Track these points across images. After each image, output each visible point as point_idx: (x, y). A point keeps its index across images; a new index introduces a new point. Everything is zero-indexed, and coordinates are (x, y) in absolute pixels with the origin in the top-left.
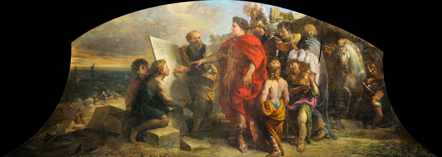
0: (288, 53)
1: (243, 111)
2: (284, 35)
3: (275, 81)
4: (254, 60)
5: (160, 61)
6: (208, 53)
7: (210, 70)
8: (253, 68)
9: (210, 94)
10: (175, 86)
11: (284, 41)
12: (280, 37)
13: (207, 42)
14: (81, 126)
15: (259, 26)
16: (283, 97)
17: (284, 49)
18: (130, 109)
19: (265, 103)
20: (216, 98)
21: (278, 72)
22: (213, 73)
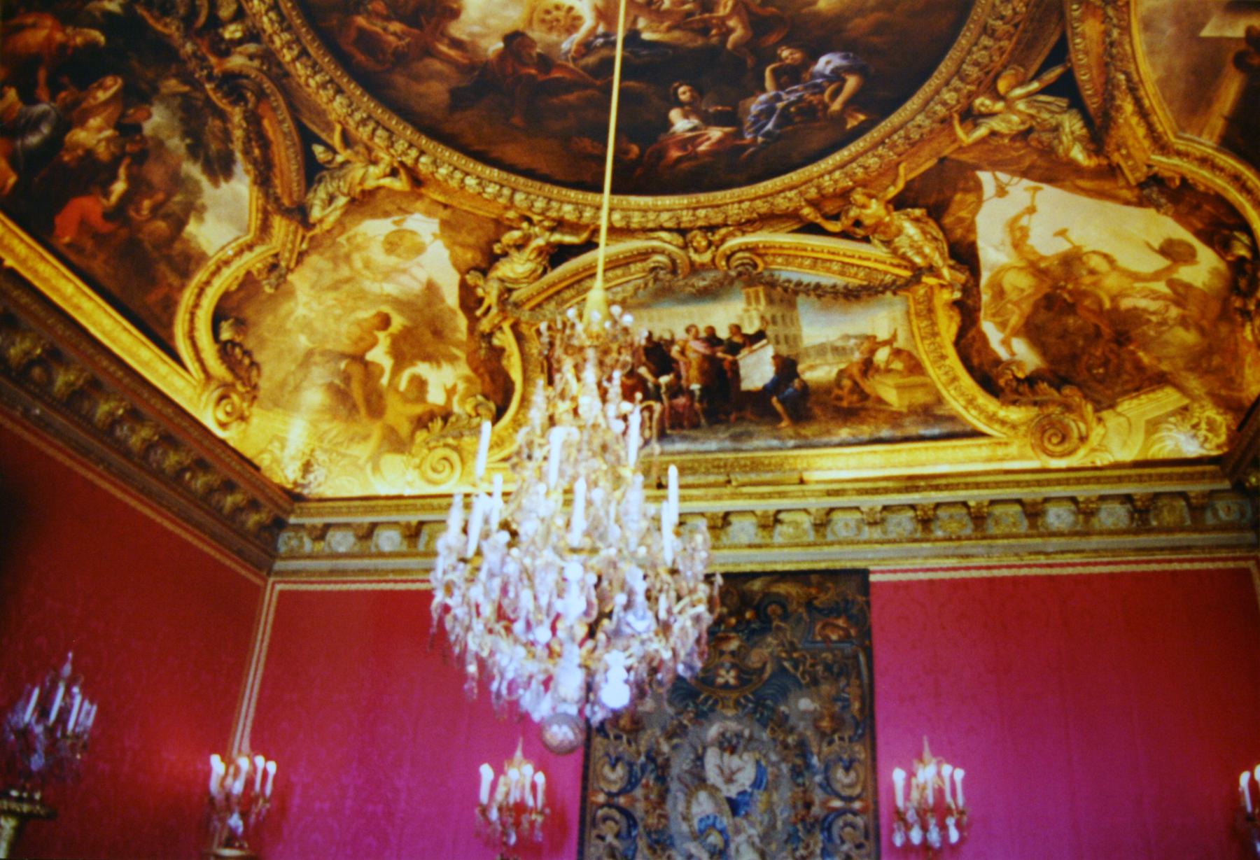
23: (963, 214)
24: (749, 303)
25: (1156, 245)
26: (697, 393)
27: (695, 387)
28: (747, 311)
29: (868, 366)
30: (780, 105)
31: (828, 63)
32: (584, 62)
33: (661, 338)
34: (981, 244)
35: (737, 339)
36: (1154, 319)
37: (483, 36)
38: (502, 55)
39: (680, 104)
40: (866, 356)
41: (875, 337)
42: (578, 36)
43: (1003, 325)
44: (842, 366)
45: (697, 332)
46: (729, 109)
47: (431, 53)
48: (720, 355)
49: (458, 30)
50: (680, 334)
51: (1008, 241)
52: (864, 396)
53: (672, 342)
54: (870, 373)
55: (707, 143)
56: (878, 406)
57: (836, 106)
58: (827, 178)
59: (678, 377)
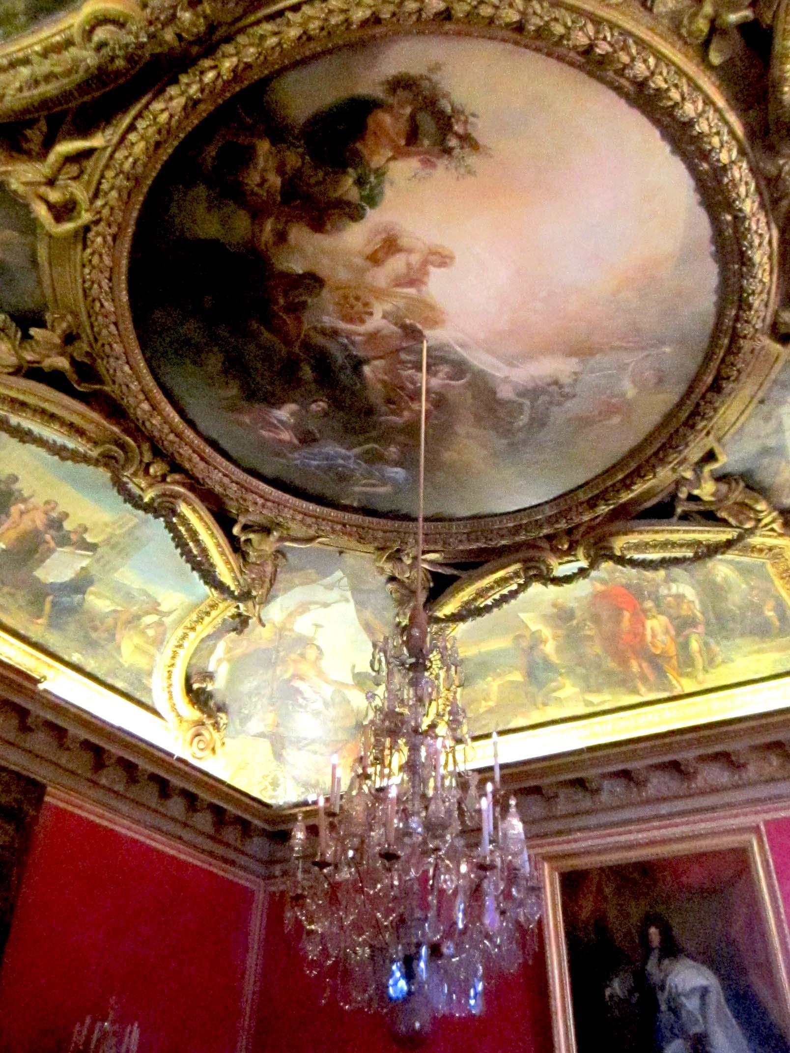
6: (578, 613)
10: (559, 650)
13: (573, 604)
14: (491, 704)
16: (667, 632)
17: (650, 589)
21: (654, 610)
22: (590, 629)
23: (297, 581)
24: (114, 523)
25: (356, 671)
28: (106, 525)
30: (341, 461)
32: (312, 333)
33: (20, 491)
34: (279, 600)
35: (74, 537)
39: (305, 407)
41: (159, 605)
42: (342, 325)
43: (229, 650)
44: (119, 608)
45: (53, 509)
47: (258, 214)
48: (48, 537)
50: (38, 501)
52: (112, 637)
53: (24, 500)
57: (357, 489)
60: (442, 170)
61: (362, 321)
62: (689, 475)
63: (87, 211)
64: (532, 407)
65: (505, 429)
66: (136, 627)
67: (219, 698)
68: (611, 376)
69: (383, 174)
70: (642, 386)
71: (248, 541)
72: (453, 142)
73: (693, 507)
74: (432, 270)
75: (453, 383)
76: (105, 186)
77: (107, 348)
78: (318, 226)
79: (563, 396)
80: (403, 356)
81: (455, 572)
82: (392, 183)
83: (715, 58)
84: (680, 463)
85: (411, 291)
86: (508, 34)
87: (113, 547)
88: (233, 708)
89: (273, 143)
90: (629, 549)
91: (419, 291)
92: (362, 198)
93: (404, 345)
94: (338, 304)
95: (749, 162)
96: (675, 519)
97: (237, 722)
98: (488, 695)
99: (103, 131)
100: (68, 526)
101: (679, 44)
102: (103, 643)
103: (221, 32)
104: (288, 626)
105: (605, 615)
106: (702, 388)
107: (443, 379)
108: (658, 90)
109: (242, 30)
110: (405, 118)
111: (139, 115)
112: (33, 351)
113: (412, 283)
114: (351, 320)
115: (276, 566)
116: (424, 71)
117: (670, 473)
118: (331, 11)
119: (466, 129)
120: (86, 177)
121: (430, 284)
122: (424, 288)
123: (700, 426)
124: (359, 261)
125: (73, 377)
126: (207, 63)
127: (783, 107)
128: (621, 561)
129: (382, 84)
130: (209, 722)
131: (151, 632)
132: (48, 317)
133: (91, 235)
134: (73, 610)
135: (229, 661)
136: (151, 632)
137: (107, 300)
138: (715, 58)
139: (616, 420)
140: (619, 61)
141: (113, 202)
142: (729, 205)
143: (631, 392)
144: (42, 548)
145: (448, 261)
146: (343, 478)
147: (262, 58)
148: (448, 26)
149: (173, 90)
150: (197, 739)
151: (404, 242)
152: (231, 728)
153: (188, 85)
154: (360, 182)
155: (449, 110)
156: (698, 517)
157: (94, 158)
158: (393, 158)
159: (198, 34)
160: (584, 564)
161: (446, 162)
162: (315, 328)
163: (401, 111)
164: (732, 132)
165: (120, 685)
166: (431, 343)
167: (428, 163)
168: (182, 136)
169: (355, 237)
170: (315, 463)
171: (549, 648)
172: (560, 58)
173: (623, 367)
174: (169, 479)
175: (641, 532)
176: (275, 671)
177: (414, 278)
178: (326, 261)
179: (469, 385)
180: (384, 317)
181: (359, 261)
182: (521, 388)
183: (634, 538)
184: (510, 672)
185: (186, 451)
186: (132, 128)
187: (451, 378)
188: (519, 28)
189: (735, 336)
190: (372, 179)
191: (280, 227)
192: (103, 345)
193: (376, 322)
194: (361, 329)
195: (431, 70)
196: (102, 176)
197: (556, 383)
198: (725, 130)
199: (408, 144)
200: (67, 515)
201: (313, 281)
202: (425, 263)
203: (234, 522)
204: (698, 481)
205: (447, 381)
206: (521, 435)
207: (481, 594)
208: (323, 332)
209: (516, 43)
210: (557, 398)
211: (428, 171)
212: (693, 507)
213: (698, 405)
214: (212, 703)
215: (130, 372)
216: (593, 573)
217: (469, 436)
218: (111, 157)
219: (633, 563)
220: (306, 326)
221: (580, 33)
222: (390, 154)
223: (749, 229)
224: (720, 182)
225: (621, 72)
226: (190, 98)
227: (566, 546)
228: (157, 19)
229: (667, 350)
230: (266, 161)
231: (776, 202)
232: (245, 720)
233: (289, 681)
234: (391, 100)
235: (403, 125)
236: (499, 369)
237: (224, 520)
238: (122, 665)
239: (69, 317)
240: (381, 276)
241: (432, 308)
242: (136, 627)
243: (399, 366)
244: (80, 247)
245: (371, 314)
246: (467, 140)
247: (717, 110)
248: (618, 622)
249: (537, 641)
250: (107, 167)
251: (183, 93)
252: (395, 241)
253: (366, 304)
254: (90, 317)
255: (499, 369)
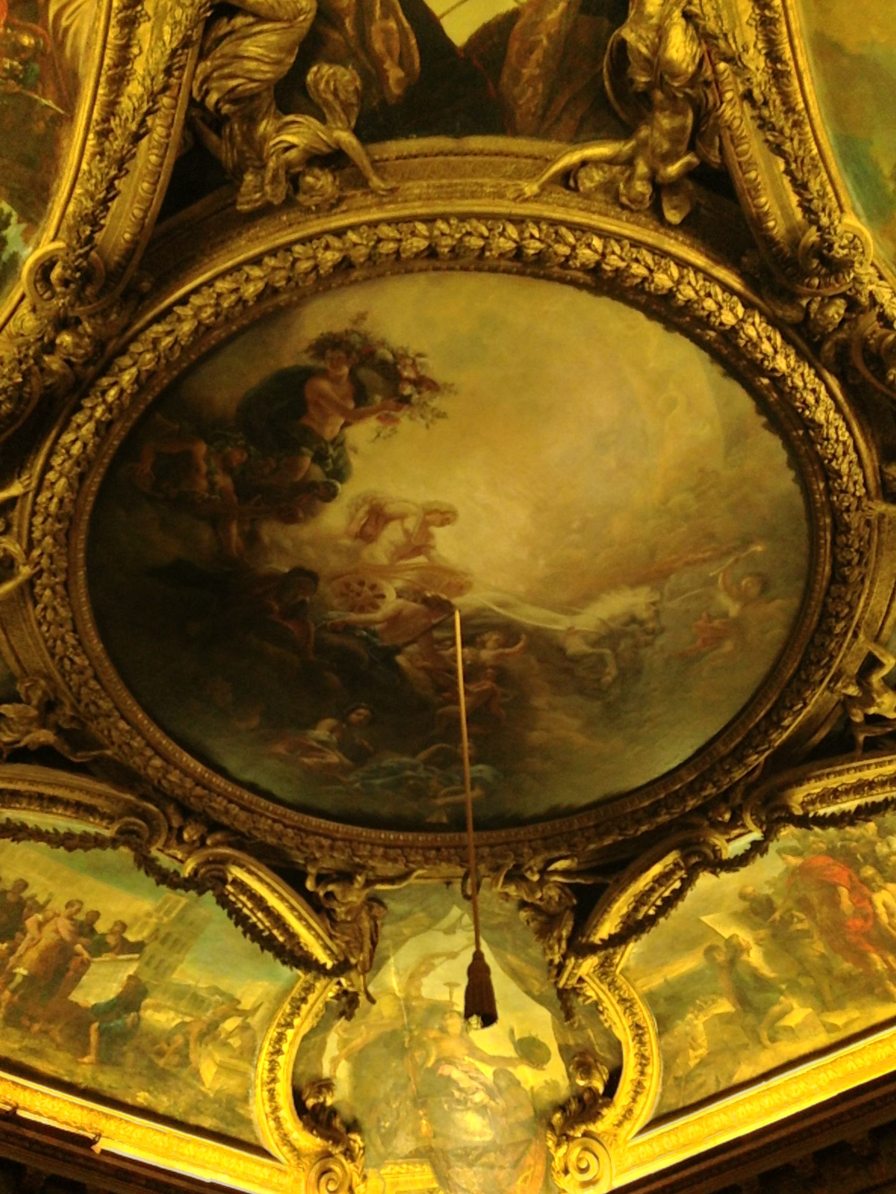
0: (874, 851)
1: (870, 948)
2: (853, 835)
3: (883, 891)
4: (836, 880)
5: (731, 937)
6: (778, 901)
7: (795, 920)
8: (844, 892)
9: (815, 946)
10: (769, 956)
11: (857, 841)
12: (850, 840)
13: (768, 891)
14: (702, 1052)
15: (814, 842)
17: (864, 850)
18: (739, 1007)
19: (889, 924)
20: (825, 947)
21: (878, 879)
22: (801, 921)
23: (406, 931)
24: (158, 910)
25: (517, 1037)
26: (18, 979)
27: (22, 971)
28: (149, 915)
29: (210, 1032)
30: (409, 773)
31: (481, 771)
34: (392, 960)
35: (111, 940)
36: (457, 1094)
37: (282, 550)
38: (274, 577)
39: (343, 717)
40: (216, 1018)
41: (239, 1002)
42: (354, 617)
43: (344, 1043)
44: (188, 1019)
45: (79, 910)
46: (371, 749)
47: (217, 521)
48: (79, 947)
49: (271, 531)
50: (58, 905)
51: (409, 972)
52: (185, 1061)
53: (41, 908)
54: (208, 1038)
55: (315, 760)
56: (190, 1080)
57: (440, 802)
58: (368, 847)
59: (12, 951)
60: (405, 422)
61: (376, 607)
62: (853, 691)
63: (25, 565)
64: (617, 656)
65: (591, 689)
66: (215, 1038)
67: (345, 1112)
68: (697, 597)
69: (342, 444)
70: (743, 598)
71: (330, 895)
72: (408, 390)
73: (878, 731)
74: (437, 531)
75: (507, 650)
76: (37, 535)
77: (93, 708)
78: (290, 517)
79: (648, 634)
80: (437, 634)
81: (600, 879)
82: (355, 451)
83: (673, 217)
84: (836, 678)
85: (421, 560)
86: (424, 264)
87: (163, 942)
88: (367, 1124)
89: (209, 443)
90: (813, 802)
91: (429, 558)
92: (328, 475)
93: (435, 621)
94: (342, 595)
95: (762, 314)
96: (859, 752)
97: (378, 1142)
98: (694, 1039)
99: (19, 477)
100: (101, 927)
101: (625, 214)
102: (174, 1070)
103: (112, 346)
104: (413, 993)
105: (814, 898)
106: (822, 583)
107: (495, 649)
108: (617, 270)
109: (134, 339)
110: (345, 378)
111: (51, 453)
112: (11, 730)
113: (417, 551)
114: (362, 610)
115: (374, 918)
116: (347, 325)
117: (827, 693)
118: (219, 295)
119: (417, 373)
120: (15, 529)
121: (438, 548)
122: (433, 553)
123: (839, 628)
124: (347, 542)
125: (64, 749)
126: (105, 381)
127: (778, 243)
128: (804, 822)
129: (306, 351)
130: (337, 1151)
131: (235, 1042)
132: (20, 688)
133: (37, 590)
134: (125, 1035)
135: (348, 1058)
136: (235, 1042)
137: (78, 655)
138: (673, 217)
139: (728, 646)
140: (556, 253)
141: (50, 549)
142: (758, 368)
143: (734, 609)
144: (74, 964)
145: (448, 516)
146: (419, 792)
147: (163, 361)
148: (355, 274)
149: (79, 418)
150: (324, 1179)
151: (391, 509)
152: (372, 1152)
153: (93, 408)
154: (320, 458)
155: (390, 357)
156: (889, 743)
157: (18, 506)
158: (346, 425)
159: (86, 354)
160: (757, 835)
161: (408, 412)
162: (324, 627)
163: (339, 373)
164: (726, 288)
165: (207, 1123)
166: (466, 611)
167: (388, 419)
168: (106, 461)
169: (335, 518)
170: (378, 782)
171: (755, 957)
172: (494, 270)
173: (712, 582)
174: (209, 842)
175: (819, 778)
176: (412, 1058)
177: (418, 545)
178: (310, 552)
179: (528, 648)
180: (399, 595)
181: (347, 542)
182: (593, 637)
183: (814, 787)
184: (714, 1002)
185: (220, 803)
186: (47, 467)
187: (504, 645)
188: (431, 253)
189: (836, 513)
190: (331, 451)
191: (247, 528)
192: (87, 705)
193: (391, 603)
194: (378, 615)
195: (355, 322)
196: (31, 525)
197: (633, 620)
198: (717, 290)
199: (358, 405)
200: (96, 915)
201: (304, 577)
202: (425, 525)
203: (304, 875)
204: (867, 698)
205: (501, 650)
206: (616, 691)
207: (642, 899)
208: (335, 629)
209: (436, 269)
210: (643, 638)
211: (389, 427)
212: (878, 731)
213: (825, 605)
214: (337, 1123)
215: (127, 727)
216: (773, 846)
217: (553, 708)
218: (35, 503)
219: (824, 822)
220: (313, 629)
221: (502, 240)
222: (342, 421)
223: (795, 388)
224: (737, 346)
225: (564, 265)
226: (99, 422)
227: (727, 816)
228: (26, 356)
229: (759, 548)
230: (208, 462)
231: (816, 348)
232: (388, 1136)
233: (433, 1071)
234: (322, 364)
235: (346, 387)
236: (556, 621)
237: (292, 877)
238: (205, 1096)
239: (42, 682)
240: (379, 552)
241: (452, 572)
242: (215, 1038)
243: (436, 646)
244: (30, 606)
245: (383, 596)
246: (422, 383)
247: (697, 270)
248: (834, 902)
249: (735, 950)
250: (33, 514)
251: (90, 418)
252: (381, 509)
253: (373, 587)
254: (63, 676)
255: (556, 621)
